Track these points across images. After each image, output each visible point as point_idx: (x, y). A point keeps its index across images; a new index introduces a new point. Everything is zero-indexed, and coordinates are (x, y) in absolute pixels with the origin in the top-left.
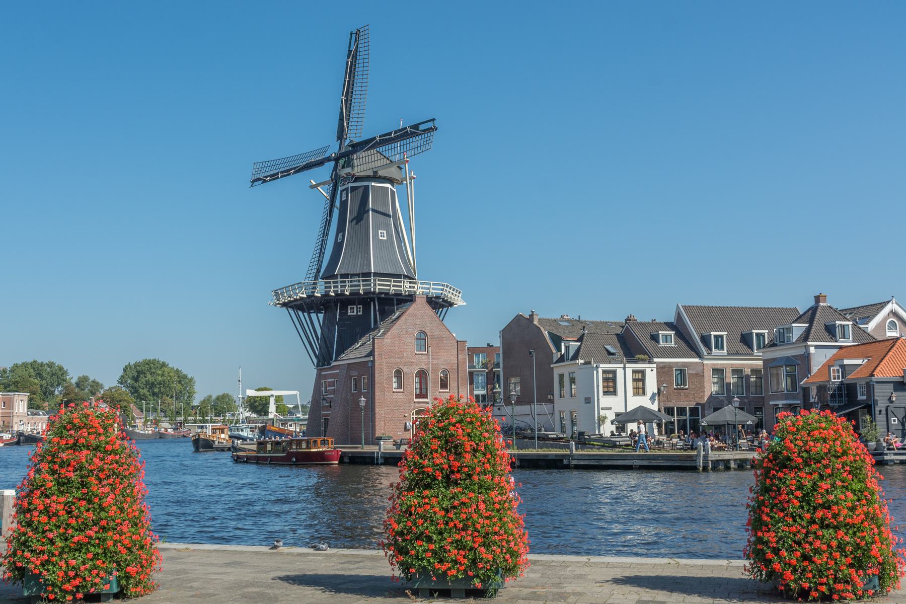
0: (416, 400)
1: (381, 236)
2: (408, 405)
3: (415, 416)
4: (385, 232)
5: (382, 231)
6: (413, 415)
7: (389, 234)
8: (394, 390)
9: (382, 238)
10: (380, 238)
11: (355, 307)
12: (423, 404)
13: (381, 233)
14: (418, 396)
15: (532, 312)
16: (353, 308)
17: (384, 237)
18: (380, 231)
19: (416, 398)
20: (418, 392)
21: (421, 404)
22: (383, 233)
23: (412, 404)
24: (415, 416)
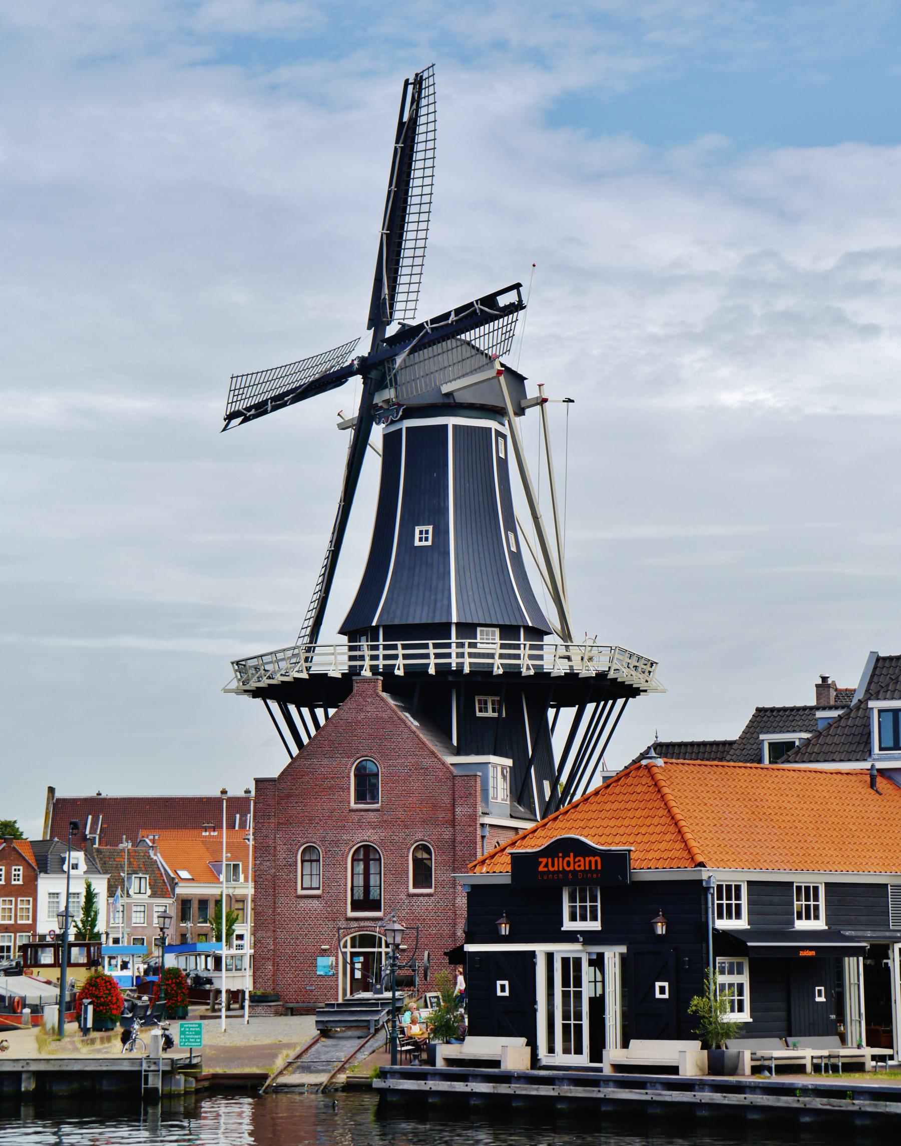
0: (351, 914)
2: (330, 924)
3: (349, 950)
4: (430, 528)
5: (424, 528)
6: (345, 946)
8: (300, 892)
12: (367, 924)
13: (421, 533)
14: (356, 906)
15: (824, 679)
18: (417, 529)
19: (354, 909)
20: (360, 894)
21: (362, 924)
22: (427, 532)
23: (342, 924)
24: (349, 950)
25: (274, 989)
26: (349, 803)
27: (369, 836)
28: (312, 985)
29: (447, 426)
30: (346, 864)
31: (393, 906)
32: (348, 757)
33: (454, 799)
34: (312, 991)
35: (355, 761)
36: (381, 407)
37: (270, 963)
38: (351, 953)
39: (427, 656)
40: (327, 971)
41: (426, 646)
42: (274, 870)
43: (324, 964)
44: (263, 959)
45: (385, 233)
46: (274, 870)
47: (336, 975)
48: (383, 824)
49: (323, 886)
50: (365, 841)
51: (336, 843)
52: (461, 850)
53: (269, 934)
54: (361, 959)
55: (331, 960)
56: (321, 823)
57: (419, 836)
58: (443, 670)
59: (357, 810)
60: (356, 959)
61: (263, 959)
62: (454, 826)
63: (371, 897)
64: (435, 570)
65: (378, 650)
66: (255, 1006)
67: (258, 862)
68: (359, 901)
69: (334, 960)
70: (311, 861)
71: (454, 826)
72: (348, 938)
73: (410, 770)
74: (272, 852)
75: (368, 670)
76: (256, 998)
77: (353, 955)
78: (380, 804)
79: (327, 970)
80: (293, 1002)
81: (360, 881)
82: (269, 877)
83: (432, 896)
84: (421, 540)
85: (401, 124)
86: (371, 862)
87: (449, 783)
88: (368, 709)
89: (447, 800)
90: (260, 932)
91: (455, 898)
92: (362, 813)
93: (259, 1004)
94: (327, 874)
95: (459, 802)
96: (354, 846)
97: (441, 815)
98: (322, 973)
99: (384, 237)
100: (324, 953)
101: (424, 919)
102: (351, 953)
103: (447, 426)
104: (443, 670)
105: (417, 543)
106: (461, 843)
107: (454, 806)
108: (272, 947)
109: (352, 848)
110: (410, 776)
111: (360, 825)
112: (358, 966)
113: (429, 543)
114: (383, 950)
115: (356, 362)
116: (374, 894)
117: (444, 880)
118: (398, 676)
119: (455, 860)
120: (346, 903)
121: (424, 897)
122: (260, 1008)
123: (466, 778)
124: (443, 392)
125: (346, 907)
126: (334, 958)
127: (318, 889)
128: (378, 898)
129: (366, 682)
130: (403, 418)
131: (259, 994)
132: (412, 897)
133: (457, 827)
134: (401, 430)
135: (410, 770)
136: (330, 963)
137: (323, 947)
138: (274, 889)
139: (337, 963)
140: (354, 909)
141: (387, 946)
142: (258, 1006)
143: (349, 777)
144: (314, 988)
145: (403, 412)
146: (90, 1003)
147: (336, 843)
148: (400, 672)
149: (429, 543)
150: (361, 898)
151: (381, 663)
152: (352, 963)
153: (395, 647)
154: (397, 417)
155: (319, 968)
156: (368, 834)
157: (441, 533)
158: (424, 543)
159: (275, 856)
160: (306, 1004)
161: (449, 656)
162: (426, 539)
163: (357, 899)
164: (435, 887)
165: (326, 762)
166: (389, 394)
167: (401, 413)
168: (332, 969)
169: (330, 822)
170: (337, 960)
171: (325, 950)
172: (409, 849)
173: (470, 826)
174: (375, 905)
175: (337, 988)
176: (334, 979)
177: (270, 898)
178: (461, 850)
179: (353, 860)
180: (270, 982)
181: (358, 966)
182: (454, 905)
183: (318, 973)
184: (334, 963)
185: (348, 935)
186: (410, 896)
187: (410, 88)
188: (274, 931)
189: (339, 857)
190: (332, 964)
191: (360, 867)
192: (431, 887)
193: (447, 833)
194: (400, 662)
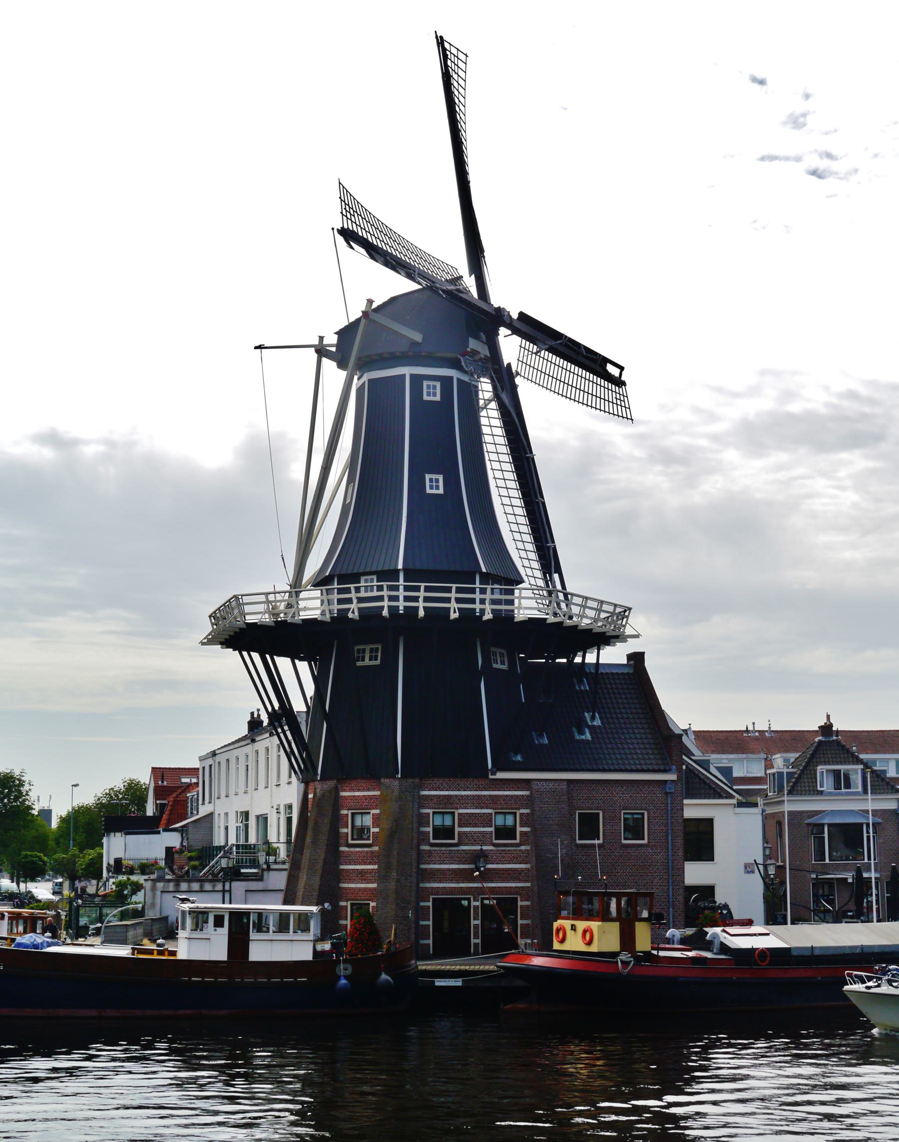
1: (431, 488)
4: (441, 478)
5: (434, 476)
7: (452, 483)
9: (434, 491)
10: (428, 491)
11: (368, 648)
16: (364, 651)
18: (428, 477)
39: (448, 600)
41: (449, 590)
58: (468, 616)
65: (475, 593)
75: (356, 613)
104: (468, 616)
105: (428, 491)
113: (441, 491)
118: (456, 619)
151: (401, 604)
153: (417, 589)
161: (473, 601)
194: (354, 606)
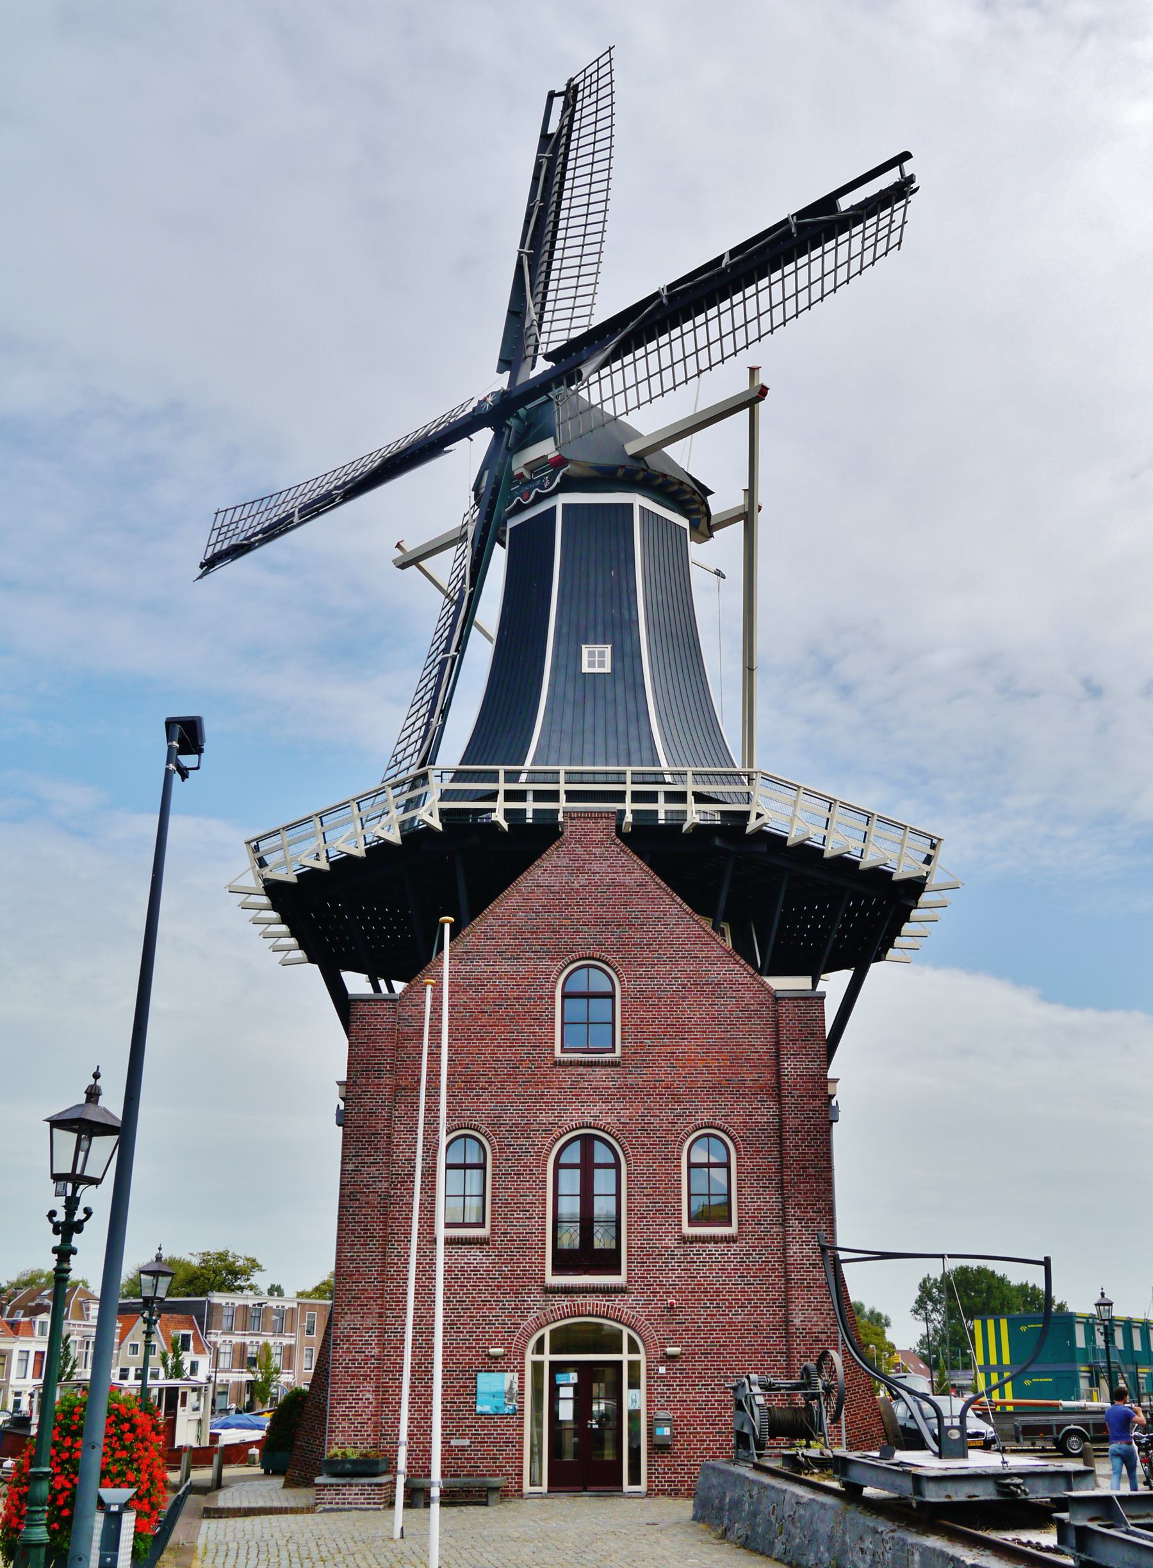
2: (509, 1301)
3: (547, 1357)
4: (608, 649)
5: (597, 648)
6: (539, 1349)
12: (591, 1300)
13: (591, 654)
14: (564, 1262)
17: (602, 665)
18: (585, 650)
19: (558, 1269)
20: (570, 1238)
21: (580, 1299)
22: (602, 654)
23: (535, 1300)
24: (547, 1357)
25: (375, 1446)
26: (553, 1047)
27: (595, 1113)
28: (463, 1436)
29: (632, 505)
30: (544, 1172)
31: (644, 1259)
32: (552, 959)
33: (777, 1044)
34: (462, 1449)
35: (566, 966)
36: (521, 475)
37: (370, 1386)
38: (552, 1363)
40: (501, 1404)
42: (386, 1185)
43: (494, 1389)
44: (353, 1376)
45: (526, 253)
46: (386, 1185)
47: (518, 1412)
48: (627, 1092)
49: (493, 1220)
50: (587, 1127)
51: (525, 1130)
52: (796, 1147)
53: (369, 1322)
54: (573, 1377)
55: (507, 1380)
56: (493, 1088)
57: (704, 1117)
59: (571, 1064)
60: (560, 1379)
61: (353, 1376)
62: (778, 1099)
63: (598, 1244)
64: (621, 708)
66: (344, 1485)
67: (350, 1167)
68: (570, 1252)
69: (516, 1380)
70: (465, 1167)
71: (778, 1099)
72: (546, 1331)
73: (684, 986)
74: (382, 1145)
76: (348, 1466)
77: (556, 1367)
78: (618, 1053)
79: (499, 1402)
80: (459, 1476)
81: (570, 1207)
82: (374, 1199)
83: (735, 1242)
84: (591, 664)
85: (545, 137)
86: (597, 1172)
87: (767, 1013)
88: (595, 867)
89: (761, 1045)
90: (348, 1317)
91: (785, 1248)
92: (581, 1070)
93: (355, 1481)
94: (503, 1194)
95: (788, 1049)
96: (562, 1136)
97: (750, 1076)
98: (487, 1409)
99: (525, 258)
100: (493, 1364)
101: (718, 1291)
102: (552, 1363)
103: (632, 505)
105: (586, 669)
106: (797, 1132)
107: (777, 1058)
108: (376, 1351)
109: (557, 1140)
110: (684, 998)
111: (577, 1094)
112: (567, 1392)
113: (607, 669)
114: (625, 1357)
115: (489, 399)
116: (602, 1240)
117: (759, 1209)
119: (780, 1171)
120: (543, 1256)
121: (716, 1243)
122: (355, 1490)
123: (802, 1003)
124: (629, 453)
125: (543, 1264)
126: (516, 1375)
127: (481, 1225)
128: (613, 1246)
129: (591, 818)
130: (561, 489)
131: (354, 1457)
132: (691, 1243)
133: (787, 1100)
134: (554, 508)
135: (684, 986)
136: (506, 1387)
137: (492, 1351)
138: (385, 1223)
139: (521, 1387)
140: (558, 1269)
141: (633, 1348)
142: (351, 1485)
143: (553, 998)
144: (467, 1442)
145: (561, 478)
146: (125, 1507)
147: (525, 1130)
148: (629, 818)
149: (607, 669)
150: (577, 1244)
152: (554, 1388)
154: (548, 487)
155: (480, 1398)
156: (594, 1112)
157: (627, 656)
158: (596, 670)
159: (388, 1154)
160: (466, 1480)
162: (602, 665)
163: (566, 1247)
164: (740, 1223)
165: (504, 967)
166: (545, 449)
167: (558, 480)
168: (511, 1399)
169: (509, 1087)
170: (521, 1379)
171: (496, 1357)
172: (682, 1142)
173: (814, 1097)
174: (608, 1262)
175: (521, 1443)
176: (514, 1422)
177: (374, 1244)
178: (796, 1147)
179: (558, 1166)
180: (369, 1429)
181: (567, 1392)
182: (784, 1260)
183: (479, 1409)
184: (516, 1387)
185: (548, 1324)
186: (685, 1240)
187: (558, 102)
188: (381, 1315)
189: (529, 1159)
190: (511, 1388)
191: (571, 1181)
192: (729, 1224)
193: (765, 1112)
